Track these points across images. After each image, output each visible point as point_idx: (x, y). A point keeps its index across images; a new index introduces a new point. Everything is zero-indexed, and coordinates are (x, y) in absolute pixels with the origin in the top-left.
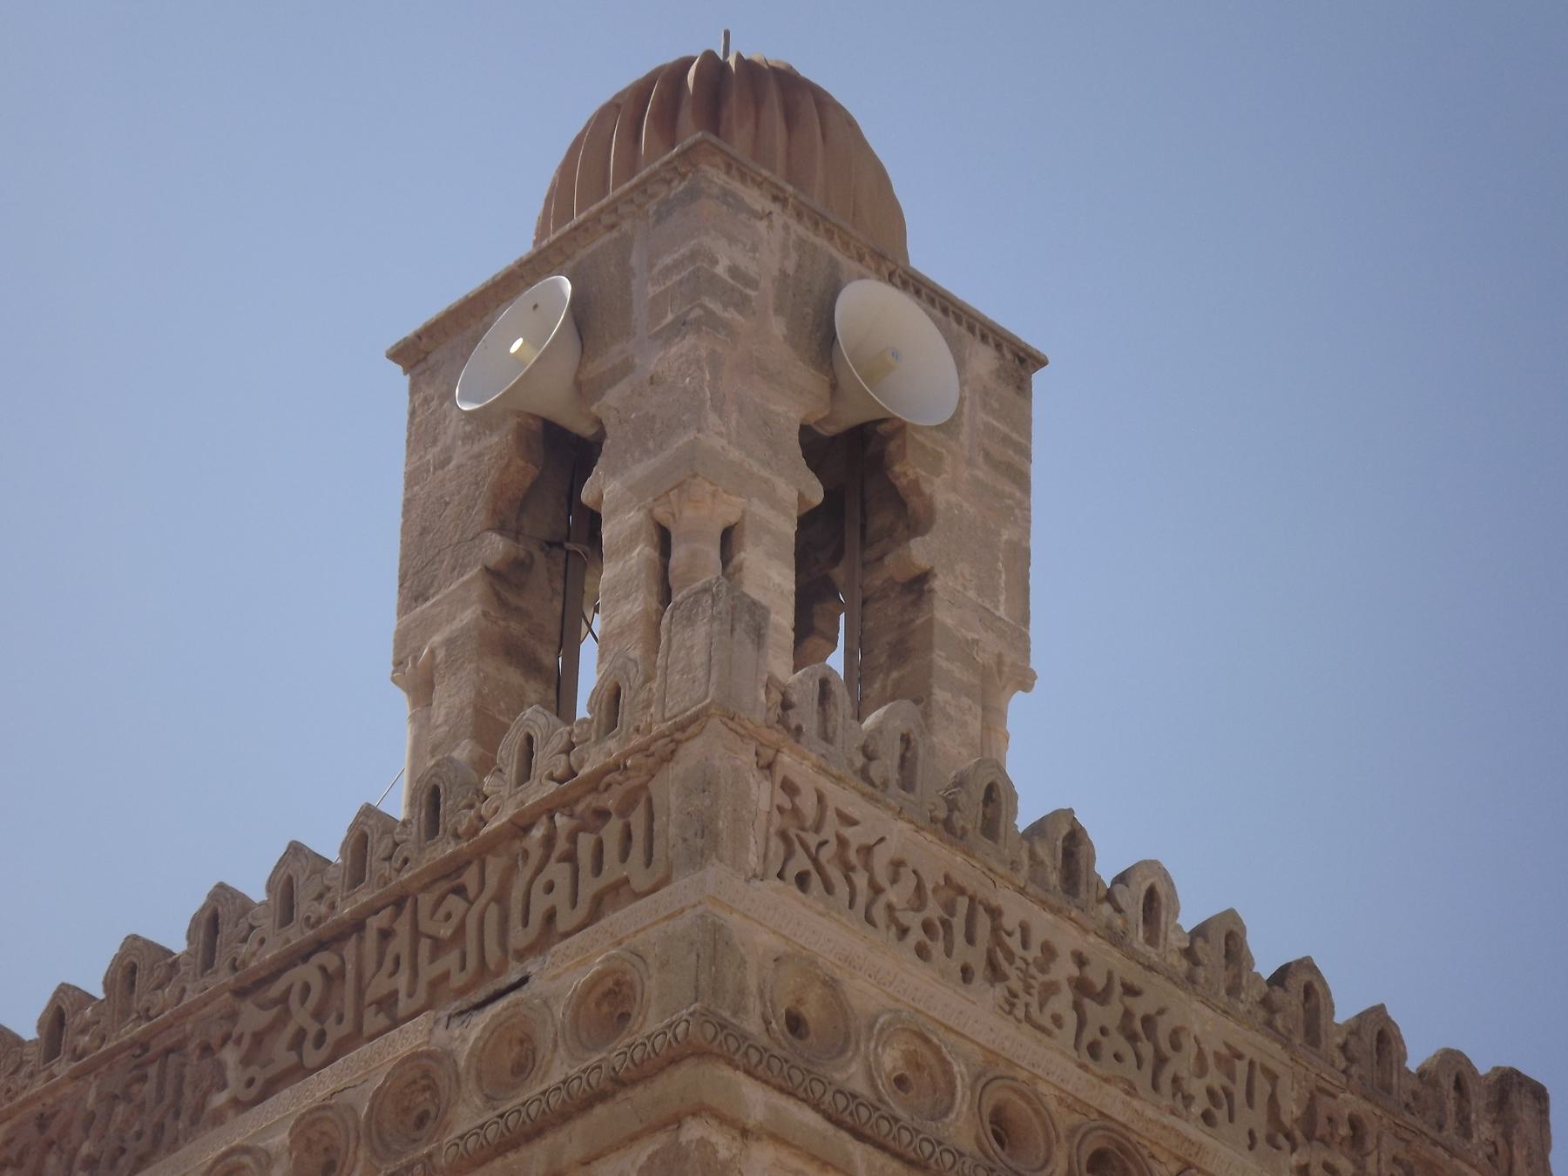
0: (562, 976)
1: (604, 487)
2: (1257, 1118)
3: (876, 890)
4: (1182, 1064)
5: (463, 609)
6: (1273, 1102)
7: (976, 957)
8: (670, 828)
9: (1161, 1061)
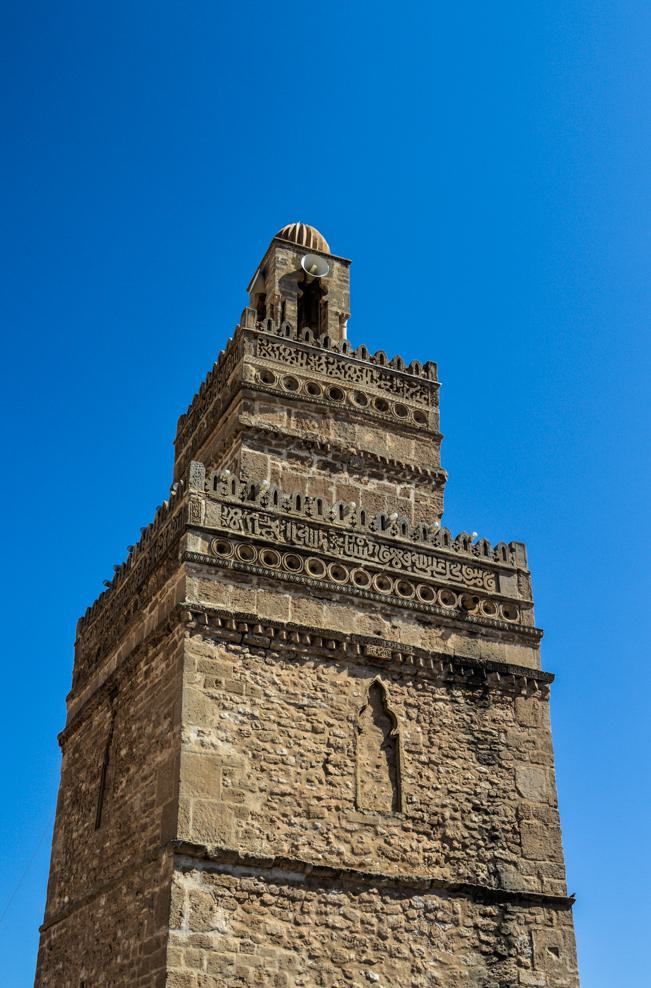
2: (369, 379)
3: (280, 354)
4: (351, 372)
6: (372, 376)
7: (304, 362)
9: (346, 373)
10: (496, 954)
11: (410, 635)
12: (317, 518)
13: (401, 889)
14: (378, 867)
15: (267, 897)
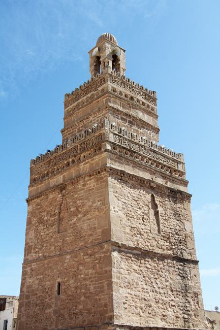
0: (100, 89)
1: (101, 60)
2: (140, 95)
5: (93, 67)
8: (106, 80)
10: (183, 276)
11: (160, 181)
12: (136, 141)
13: (162, 258)
14: (157, 251)
15: (132, 258)
